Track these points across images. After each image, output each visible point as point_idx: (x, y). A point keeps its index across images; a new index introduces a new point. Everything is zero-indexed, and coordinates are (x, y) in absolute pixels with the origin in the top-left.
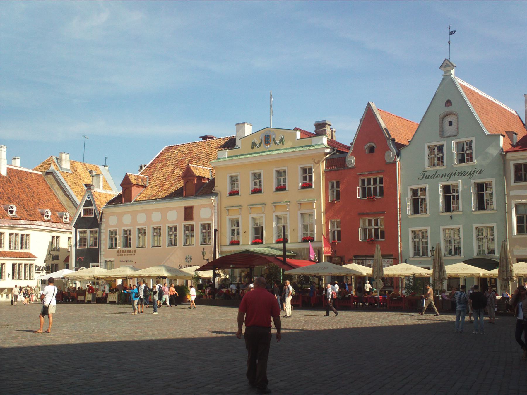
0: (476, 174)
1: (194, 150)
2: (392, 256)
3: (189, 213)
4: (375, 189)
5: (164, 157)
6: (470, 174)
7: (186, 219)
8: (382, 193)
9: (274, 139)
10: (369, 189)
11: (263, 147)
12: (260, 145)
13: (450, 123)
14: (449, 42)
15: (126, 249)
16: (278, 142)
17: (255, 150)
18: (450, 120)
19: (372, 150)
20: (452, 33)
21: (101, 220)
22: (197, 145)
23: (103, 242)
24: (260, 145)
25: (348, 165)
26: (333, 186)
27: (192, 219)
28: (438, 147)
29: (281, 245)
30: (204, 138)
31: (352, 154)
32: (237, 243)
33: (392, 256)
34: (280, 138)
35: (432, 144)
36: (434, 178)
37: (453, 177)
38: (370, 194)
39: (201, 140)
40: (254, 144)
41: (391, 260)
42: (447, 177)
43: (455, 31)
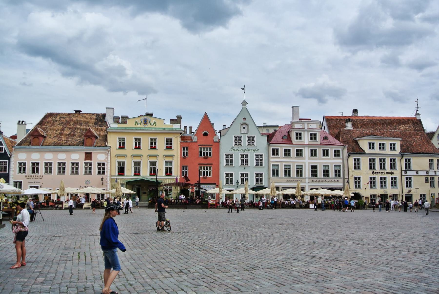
1: (74, 119)
2: (215, 184)
3: (88, 156)
4: (207, 153)
5: (50, 119)
7: (86, 159)
8: (210, 155)
9: (150, 122)
10: (204, 153)
12: (140, 124)
13: (244, 128)
15: (34, 175)
17: (137, 126)
19: (205, 134)
21: (11, 156)
22: (74, 115)
23: (12, 169)
24: (140, 124)
26: (184, 150)
27: (91, 159)
30: (76, 111)
33: (215, 184)
35: (236, 136)
38: (204, 155)
39: (74, 112)
40: (136, 123)
41: (214, 186)
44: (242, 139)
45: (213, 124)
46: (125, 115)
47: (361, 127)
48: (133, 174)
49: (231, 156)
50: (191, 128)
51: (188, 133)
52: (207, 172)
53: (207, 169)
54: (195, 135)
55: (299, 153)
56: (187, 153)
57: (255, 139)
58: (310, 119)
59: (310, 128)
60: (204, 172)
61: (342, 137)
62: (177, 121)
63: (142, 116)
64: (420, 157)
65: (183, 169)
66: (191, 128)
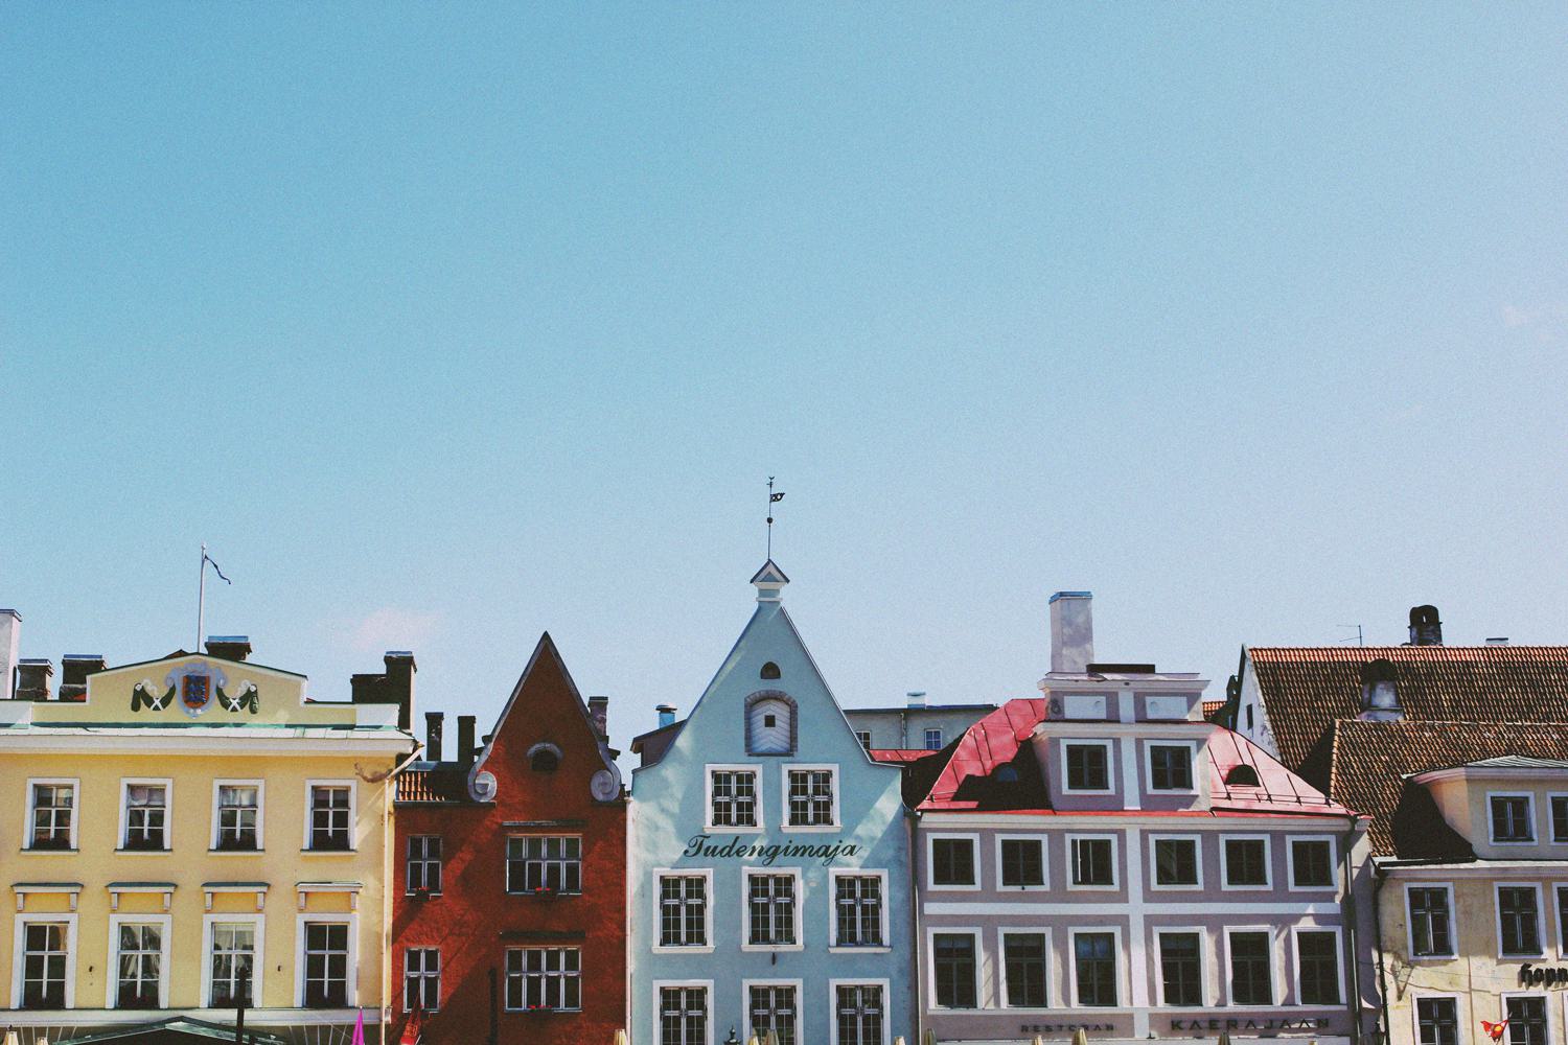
0: (840, 856)
6: (825, 854)
9: (220, 692)
11: (176, 711)
12: (166, 701)
13: (770, 721)
14: (770, 520)
16: (235, 703)
17: (146, 715)
18: (769, 713)
20: (775, 498)
25: (473, 796)
28: (740, 778)
29: (230, 1015)
31: (486, 766)
32: (56, 1001)
34: (242, 691)
36: (728, 854)
37: (780, 858)
42: (764, 857)
43: (782, 495)
44: (758, 785)
45: (600, 703)
46: (84, 649)
47: (1456, 707)
48: (111, 998)
49: (696, 886)
50: (466, 724)
51: (450, 753)
52: (553, 983)
53: (553, 964)
54: (486, 766)
55: (1095, 863)
56: (433, 869)
57: (835, 785)
58: (1150, 669)
59: (1151, 715)
60: (534, 985)
61: (1344, 768)
62: (389, 684)
63: (181, 653)
64: (1039, 814)
65: (414, 966)
66: (466, 724)
